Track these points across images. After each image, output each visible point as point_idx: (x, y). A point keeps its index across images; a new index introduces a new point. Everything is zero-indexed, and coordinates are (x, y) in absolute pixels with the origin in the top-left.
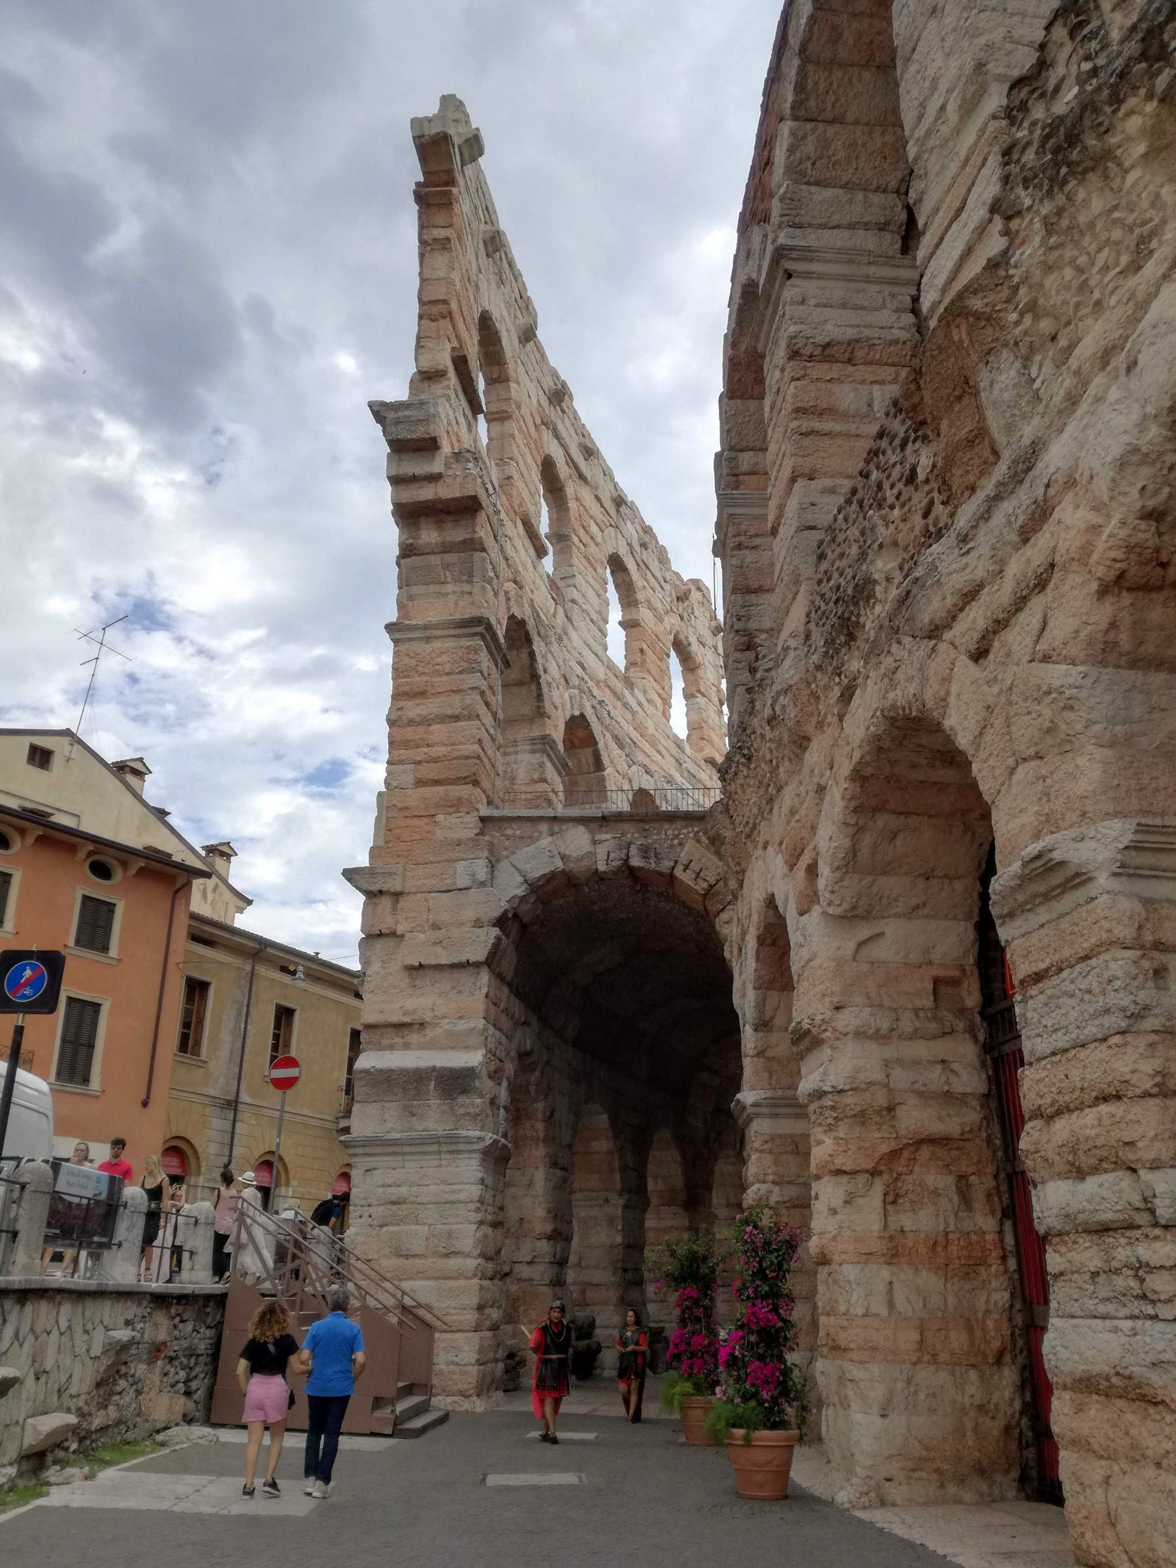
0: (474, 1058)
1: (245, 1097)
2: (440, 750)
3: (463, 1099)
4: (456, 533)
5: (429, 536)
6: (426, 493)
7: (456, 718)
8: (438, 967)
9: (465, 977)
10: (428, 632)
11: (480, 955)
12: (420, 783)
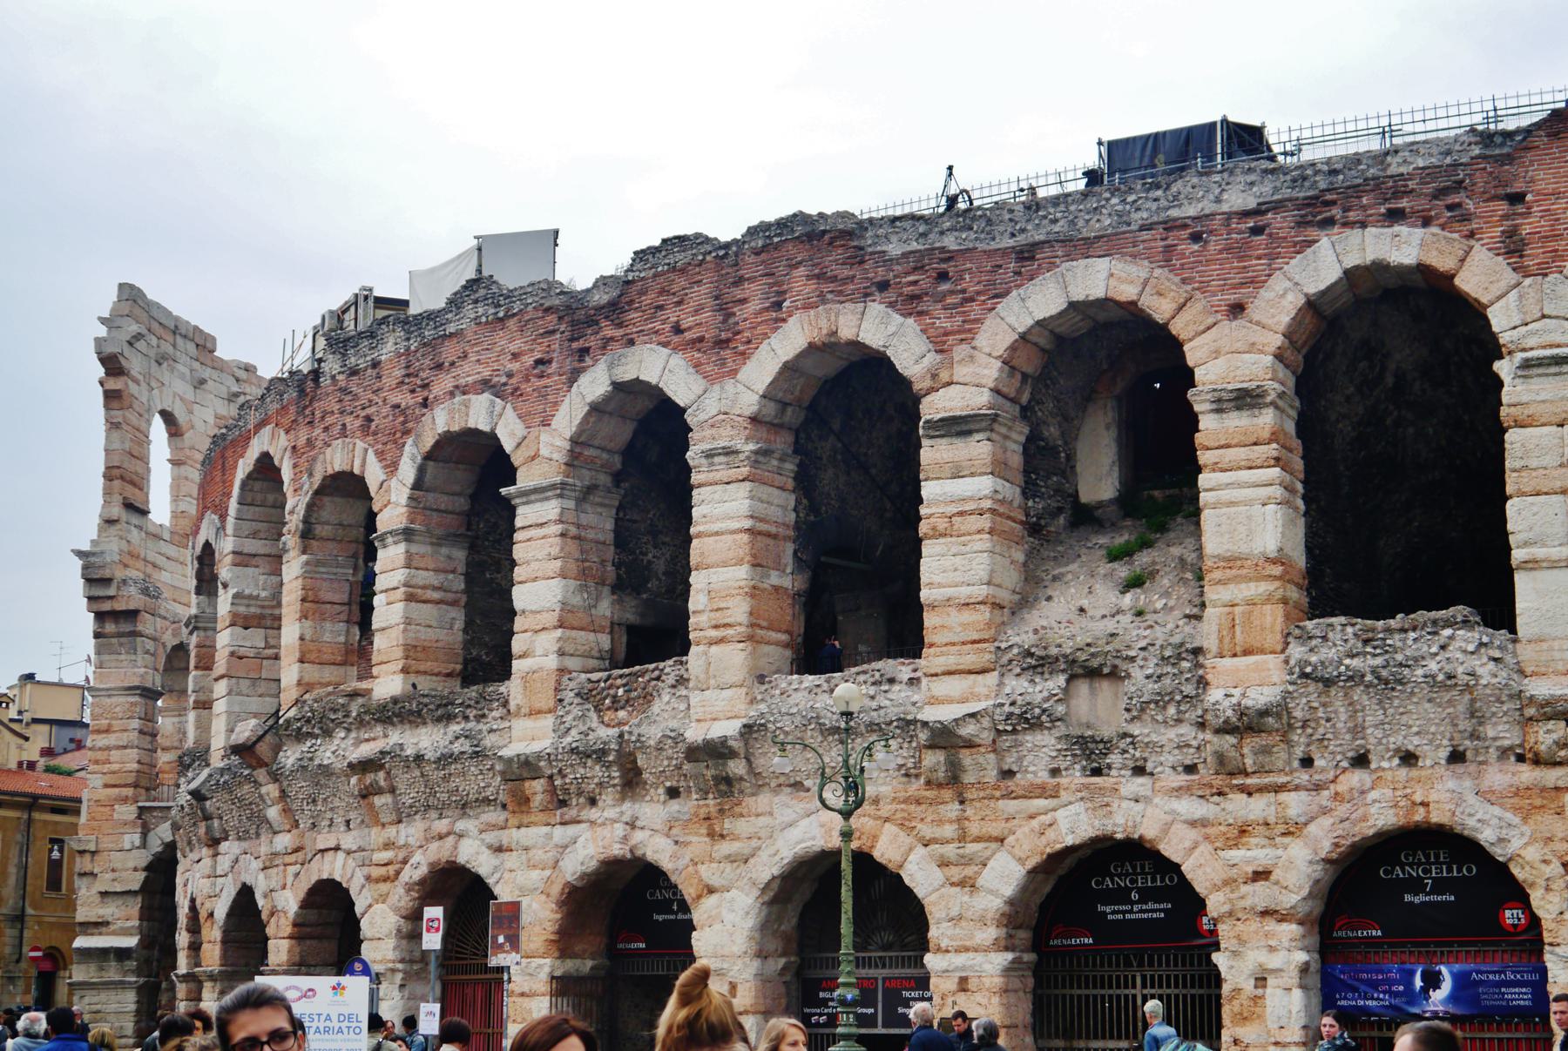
0: (131, 942)
1: (29, 911)
2: (115, 767)
3: (128, 963)
4: (126, 627)
5: (110, 627)
6: (106, 606)
7: (125, 747)
8: (116, 893)
9: (130, 900)
10: (109, 693)
11: (136, 887)
12: (106, 786)
